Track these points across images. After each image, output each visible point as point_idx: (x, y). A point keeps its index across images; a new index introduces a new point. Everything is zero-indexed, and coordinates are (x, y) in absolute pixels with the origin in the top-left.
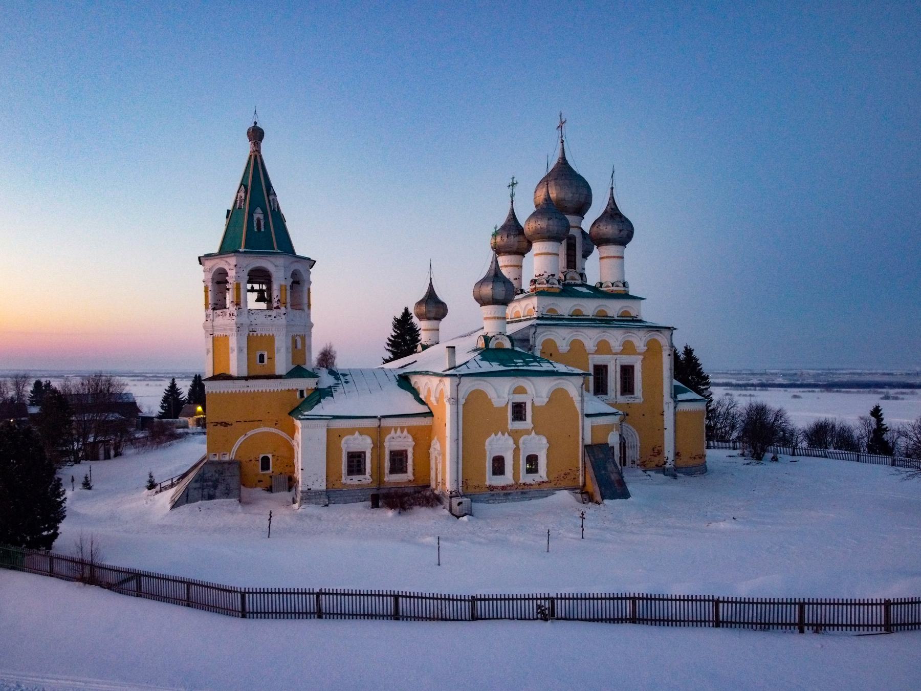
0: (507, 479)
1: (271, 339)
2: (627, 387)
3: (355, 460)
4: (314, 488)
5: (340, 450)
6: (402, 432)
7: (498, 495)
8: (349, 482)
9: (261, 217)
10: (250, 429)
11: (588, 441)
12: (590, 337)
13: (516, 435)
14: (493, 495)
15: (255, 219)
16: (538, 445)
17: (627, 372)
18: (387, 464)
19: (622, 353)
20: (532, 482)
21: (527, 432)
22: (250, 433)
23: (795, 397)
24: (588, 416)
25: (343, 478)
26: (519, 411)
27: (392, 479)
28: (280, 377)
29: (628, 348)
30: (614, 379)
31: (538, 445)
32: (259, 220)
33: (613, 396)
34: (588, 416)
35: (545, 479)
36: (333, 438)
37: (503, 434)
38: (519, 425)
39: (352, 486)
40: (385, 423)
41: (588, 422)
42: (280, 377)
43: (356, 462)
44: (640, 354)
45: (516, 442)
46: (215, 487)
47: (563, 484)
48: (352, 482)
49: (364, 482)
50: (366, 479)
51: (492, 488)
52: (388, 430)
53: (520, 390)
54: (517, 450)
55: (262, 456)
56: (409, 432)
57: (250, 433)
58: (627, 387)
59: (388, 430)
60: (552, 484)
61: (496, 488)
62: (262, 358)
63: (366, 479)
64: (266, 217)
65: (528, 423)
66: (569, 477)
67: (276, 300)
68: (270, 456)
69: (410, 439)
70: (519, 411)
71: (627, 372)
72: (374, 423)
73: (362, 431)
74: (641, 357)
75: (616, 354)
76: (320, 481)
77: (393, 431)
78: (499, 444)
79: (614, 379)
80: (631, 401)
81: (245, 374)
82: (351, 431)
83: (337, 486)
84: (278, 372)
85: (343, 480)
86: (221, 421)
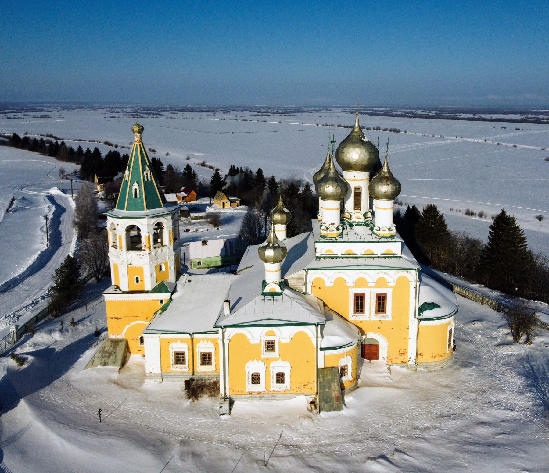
5: (169, 352)
7: (256, 397)
10: (132, 321)
11: (321, 365)
12: (350, 277)
13: (267, 362)
14: (251, 397)
18: (198, 360)
19: (375, 287)
21: (276, 360)
24: (322, 349)
26: (270, 346)
27: (202, 370)
30: (370, 304)
31: (284, 368)
33: (368, 316)
34: (322, 349)
39: (178, 372)
41: (321, 354)
43: (180, 358)
46: (109, 357)
49: (184, 370)
51: (250, 393)
52: (199, 341)
53: (273, 333)
59: (199, 341)
61: (254, 392)
64: (139, 186)
66: (307, 387)
70: (270, 346)
73: (182, 341)
77: (201, 341)
79: (370, 304)
80: (382, 319)
82: (175, 340)
85: (171, 369)
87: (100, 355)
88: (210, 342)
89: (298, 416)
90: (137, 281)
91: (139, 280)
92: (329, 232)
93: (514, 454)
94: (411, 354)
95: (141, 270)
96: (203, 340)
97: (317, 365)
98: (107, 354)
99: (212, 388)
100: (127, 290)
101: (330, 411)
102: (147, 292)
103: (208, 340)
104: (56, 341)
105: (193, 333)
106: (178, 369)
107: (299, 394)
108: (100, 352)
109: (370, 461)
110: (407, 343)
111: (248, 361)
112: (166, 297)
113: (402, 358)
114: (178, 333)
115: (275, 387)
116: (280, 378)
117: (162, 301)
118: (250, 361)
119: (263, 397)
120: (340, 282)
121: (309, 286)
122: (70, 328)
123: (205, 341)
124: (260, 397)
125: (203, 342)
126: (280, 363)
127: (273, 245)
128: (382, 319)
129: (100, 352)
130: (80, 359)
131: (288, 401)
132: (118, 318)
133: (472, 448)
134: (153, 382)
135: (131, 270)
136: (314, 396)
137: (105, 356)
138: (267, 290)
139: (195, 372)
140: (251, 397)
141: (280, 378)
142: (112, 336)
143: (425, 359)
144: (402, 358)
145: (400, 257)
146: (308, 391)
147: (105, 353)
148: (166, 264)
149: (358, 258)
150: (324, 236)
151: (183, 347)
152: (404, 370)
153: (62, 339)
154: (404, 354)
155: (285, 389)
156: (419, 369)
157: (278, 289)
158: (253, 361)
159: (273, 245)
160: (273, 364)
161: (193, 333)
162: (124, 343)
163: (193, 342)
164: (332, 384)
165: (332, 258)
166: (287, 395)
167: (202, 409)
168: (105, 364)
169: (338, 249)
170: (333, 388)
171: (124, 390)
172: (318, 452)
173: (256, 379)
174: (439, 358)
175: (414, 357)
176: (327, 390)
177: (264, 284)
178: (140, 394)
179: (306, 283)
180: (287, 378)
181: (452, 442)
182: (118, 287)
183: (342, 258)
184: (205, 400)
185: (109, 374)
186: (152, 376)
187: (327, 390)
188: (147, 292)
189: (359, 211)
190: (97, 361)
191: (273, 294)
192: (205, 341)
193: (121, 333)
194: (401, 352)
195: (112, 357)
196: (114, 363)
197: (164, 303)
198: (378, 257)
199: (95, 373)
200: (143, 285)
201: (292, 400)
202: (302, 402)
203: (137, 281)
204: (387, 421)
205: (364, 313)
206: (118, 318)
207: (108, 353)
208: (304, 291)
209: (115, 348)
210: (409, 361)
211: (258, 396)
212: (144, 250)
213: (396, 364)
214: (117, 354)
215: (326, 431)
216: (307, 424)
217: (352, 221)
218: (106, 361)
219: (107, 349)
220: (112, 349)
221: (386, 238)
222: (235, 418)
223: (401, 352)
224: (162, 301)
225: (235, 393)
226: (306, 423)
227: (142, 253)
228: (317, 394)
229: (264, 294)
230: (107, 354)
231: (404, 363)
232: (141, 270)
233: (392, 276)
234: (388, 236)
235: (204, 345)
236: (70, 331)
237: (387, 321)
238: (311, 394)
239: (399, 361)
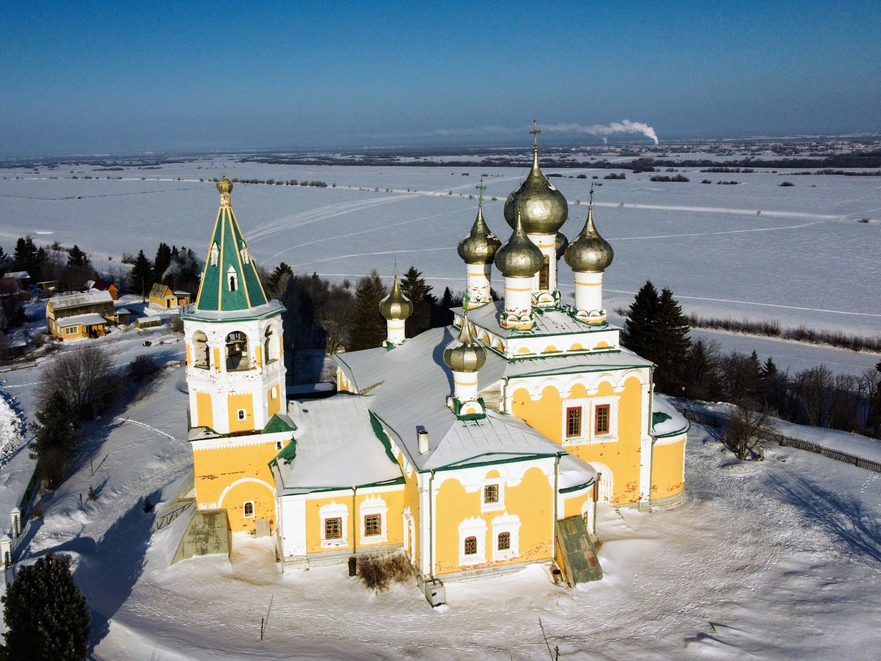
2: (602, 425)
3: (332, 525)
7: (472, 574)
8: (327, 547)
9: (235, 275)
10: (234, 480)
11: (561, 516)
14: (465, 574)
15: (229, 278)
17: (602, 412)
18: (362, 528)
19: (597, 395)
21: (500, 513)
23: (786, 184)
24: (562, 491)
25: (322, 542)
26: (491, 493)
27: (368, 544)
29: (605, 389)
30: (588, 421)
31: (510, 523)
32: (232, 278)
34: (562, 491)
35: (517, 555)
36: (312, 509)
38: (491, 507)
39: (330, 550)
40: (359, 491)
43: (333, 528)
44: (617, 394)
45: (488, 525)
49: (341, 546)
50: (343, 543)
51: (464, 569)
52: (363, 497)
53: (495, 475)
54: (489, 534)
55: (245, 503)
58: (602, 425)
59: (363, 497)
61: (469, 567)
63: (343, 543)
65: (499, 505)
66: (541, 550)
67: (252, 361)
68: (252, 502)
69: (384, 504)
71: (602, 412)
73: (339, 501)
74: (619, 397)
75: (591, 396)
78: (470, 527)
79: (588, 421)
80: (606, 441)
82: (328, 501)
83: (317, 549)
84: (257, 428)
87: (191, 538)
88: (379, 497)
89: (544, 594)
90: (241, 417)
91: (245, 415)
92: (521, 323)
93: (866, 609)
94: (644, 488)
95: (249, 398)
96: (370, 496)
97: (556, 516)
98: (202, 536)
99: (399, 568)
100: (227, 432)
101: (587, 581)
102: (258, 432)
103: (376, 495)
104: (84, 526)
105: (357, 487)
106: (333, 546)
107: (531, 562)
108: (190, 534)
109: (692, 644)
110: (638, 472)
111: (462, 519)
112: (284, 437)
113: (631, 496)
114: (334, 489)
115: (498, 555)
116: (504, 541)
117: (279, 444)
118: (466, 519)
119: (481, 572)
120: (551, 394)
121: (509, 402)
122: (91, 503)
123: (373, 497)
124: (478, 573)
126: (506, 517)
127: (472, 345)
128: (606, 441)
130: (149, 550)
131: (517, 573)
132: (212, 477)
133: (807, 607)
134: (296, 570)
135: (233, 400)
136: (551, 563)
137: (200, 539)
138: (464, 412)
140: (465, 574)
141: (504, 541)
142: (202, 507)
143: (661, 493)
144: (631, 496)
145: (619, 351)
146: (542, 556)
147: (198, 534)
148: (277, 387)
149: (565, 356)
150: (513, 329)
152: (635, 512)
153: (91, 522)
154: (634, 489)
155: (511, 556)
156: (654, 508)
157: (478, 409)
158: (469, 519)
159: (472, 345)
160: (497, 520)
161: (357, 487)
162: (223, 515)
164: (581, 541)
165: (531, 359)
166: (514, 566)
167: (400, 601)
168: (204, 552)
169: (536, 346)
170: (583, 546)
171: (260, 588)
172: (612, 640)
173: (471, 546)
174: (676, 491)
175: (646, 492)
176: (576, 551)
177: (458, 405)
178: (289, 590)
179: (505, 397)
180: (514, 541)
181: (775, 603)
182: (208, 430)
183: (543, 358)
184: (395, 587)
185: (217, 566)
186: (294, 560)
187: (576, 551)
188: (258, 432)
189: (545, 291)
190: (189, 548)
191: (474, 417)
192: (373, 497)
193: (217, 500)
194: (630, 487)
195: (212, 540)
196: (217, 548)
197: (283, 446)
198: (590, 354)
199: (193, 567)
200: (252, 422)
201: (522, 572)
202: (538, 573)
203: (241, 417)
204: (669, 586)
205: (580, 435)
206: (212, 477)
207: (204, 534)
208: (502, 409)
209: (211, 524)
210: (640, 498)
211: (474, 571)
212: (254, 368)
213: (624, 505)
214: (218, 533)
215: (598, 611)
216: (566, 603)
217: (538, 305)
218: (204, 547)
219: (200, 527)
220: (207, 526)
221: (598, 325)
222: (457, 609)
223: (630, 487)
224: (279, 444)
225: (443, 571)
226: (563, 601)
227: (250, 373)
228: (556, 559)
229: (460, 418)
230: (202, 536)
231: (635, 503)
232: (249, 398)
233: (617, 379)
234: (600, 322)
235: (373, 503)
236: (95, 508)
237: (611, 443)
238: (545, 560)
239: (627, 500)
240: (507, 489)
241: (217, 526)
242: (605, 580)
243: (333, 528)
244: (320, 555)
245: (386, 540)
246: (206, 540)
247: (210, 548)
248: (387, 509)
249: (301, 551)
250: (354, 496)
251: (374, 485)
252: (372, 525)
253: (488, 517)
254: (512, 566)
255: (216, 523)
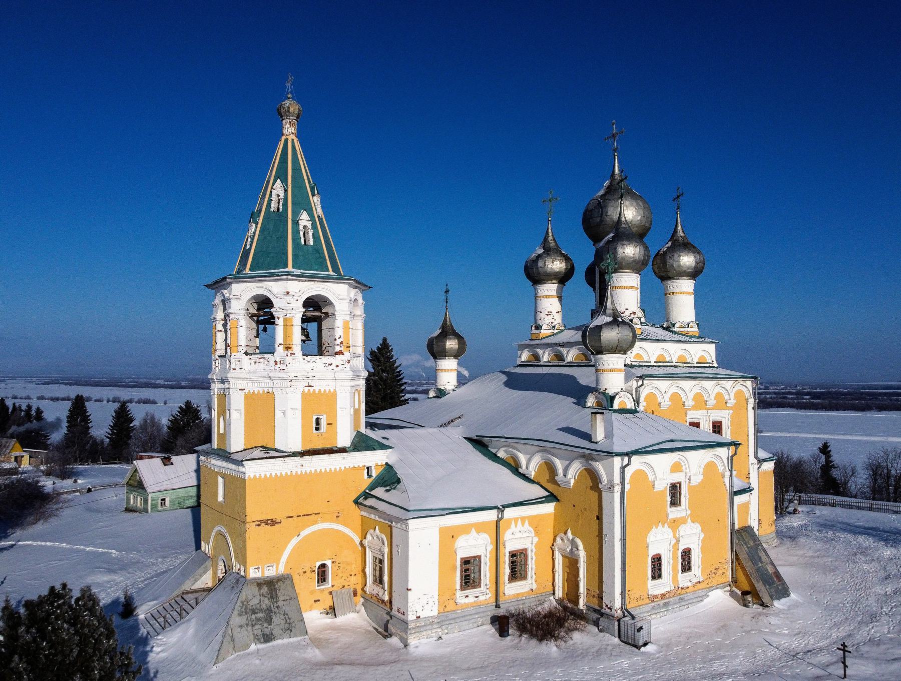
0: (664, 585)
1: (332, 397)
4: (423, 615)
6: (523, 524)
16: (692, 536)
18: (506, 570)
20: (689, 584)
22: (304, 533)
28: (343, 450)
31: (692, 536)
37: (663, 526)
38: (674, 513)
42: (343, 450)
43: (469, 573)
47: (714, 582)
48: (467, 601)
49: (482, 598)
50: (483, 594)
52: (509, 521)
56: (530, 524)
57: (304, 533)
60: (706, 582)
62: (318, 421)
63: (483, 594)
72: (492, 515)
73: (480, 527)
76: (431, 603)
81: (298, 448)
82: (465, 529)
83: (451, 606)
86: (265, 518)
98: (261, 615)
105: (505, 507)
106: (471, 599)
107: (711, 588)
125: (523, 524)
129: (240, 615)
131: (702, 603)
136: (728, 588)
137: (258, 619)
139: (502, 599)
147: (254, 612)
151: (475, 544)
155: (695, 580)
161: (505, 507)
163: (497, 527)
195: (276, 619)
201: (706, 601)
207: (261, 611)
219: (255, 602)
220: (267, 601)
230: (261, 615)
240: (691, 489)
241: (281, 598)
242: (793, 596)
243: (469, 573)
244: (454, 616)
245: (534, 587)
246: (269, 620)
247: (277, 631)
248: (536, 540)
249: (431, 610)
250: (497, 522)
251: (521, 504)
252: (518, 566)
253: (675, 524)
254: (695, 596)
255: (279, 594)
